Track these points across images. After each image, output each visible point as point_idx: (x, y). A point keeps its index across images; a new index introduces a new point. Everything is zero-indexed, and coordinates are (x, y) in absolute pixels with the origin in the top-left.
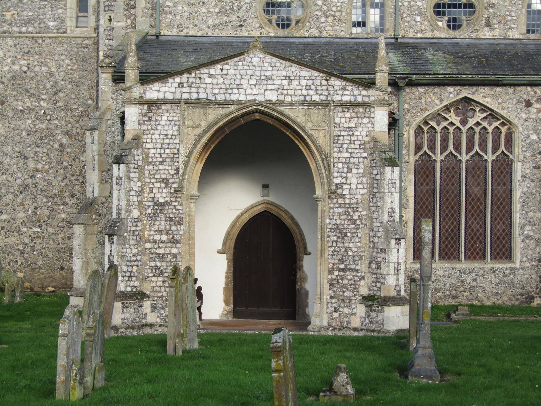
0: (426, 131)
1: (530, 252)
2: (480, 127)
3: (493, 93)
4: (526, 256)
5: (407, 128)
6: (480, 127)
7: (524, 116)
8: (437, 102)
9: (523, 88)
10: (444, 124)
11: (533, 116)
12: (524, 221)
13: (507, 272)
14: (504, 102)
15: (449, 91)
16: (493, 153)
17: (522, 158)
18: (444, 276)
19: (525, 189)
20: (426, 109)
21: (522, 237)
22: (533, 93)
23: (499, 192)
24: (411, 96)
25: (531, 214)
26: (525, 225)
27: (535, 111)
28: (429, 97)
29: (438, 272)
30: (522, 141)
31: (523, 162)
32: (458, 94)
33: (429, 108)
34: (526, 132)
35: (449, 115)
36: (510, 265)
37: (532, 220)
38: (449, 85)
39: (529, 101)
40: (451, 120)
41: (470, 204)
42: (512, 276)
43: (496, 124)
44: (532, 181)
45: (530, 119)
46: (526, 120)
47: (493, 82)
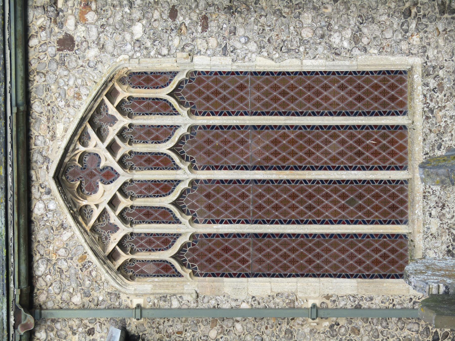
0: (130, 257)
1: (388, 35)
2: (118, 141)
3: (44, 119)
4: (398, 43)
5: (123, 297)
6: (118, 141)
7: (92, 53)
8: (66, 235)
9: (32, 54)
10: (114, 218)
11: (94, 32)
12: (320, 49)
13: (433, 83)
14: (63, 95)
15: (42, 211)
16: (176, 113)
17: (185, 54)
18: (441, 217)
19: (253, 46)
20: (83, 258)
21: (356, 52)
22: (43, 34)
23: (259, 99)
24: (54, 289)
25: (306, 34)
26: (330, 46)
27: (81, 28)
28: (56, 252)
29: (434, 230)
30: (148, 56)
31: (191, 55)
32: (49, 192)
33: (80, 253)
34: (129, 47)
35: (95, 207)
36: (417, 77)
37: (319, 32)
38: (29, 211)
39: (60, 42)
40: (104, 205)
41: (284, 159)
42: (441, 73)
43: (112, 110)
44: (233, 32)
45: (99, 38)
46: (103, 48)
47: (22, 124)
